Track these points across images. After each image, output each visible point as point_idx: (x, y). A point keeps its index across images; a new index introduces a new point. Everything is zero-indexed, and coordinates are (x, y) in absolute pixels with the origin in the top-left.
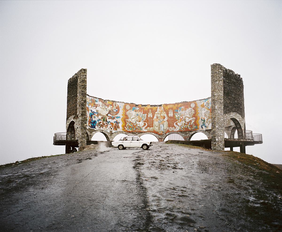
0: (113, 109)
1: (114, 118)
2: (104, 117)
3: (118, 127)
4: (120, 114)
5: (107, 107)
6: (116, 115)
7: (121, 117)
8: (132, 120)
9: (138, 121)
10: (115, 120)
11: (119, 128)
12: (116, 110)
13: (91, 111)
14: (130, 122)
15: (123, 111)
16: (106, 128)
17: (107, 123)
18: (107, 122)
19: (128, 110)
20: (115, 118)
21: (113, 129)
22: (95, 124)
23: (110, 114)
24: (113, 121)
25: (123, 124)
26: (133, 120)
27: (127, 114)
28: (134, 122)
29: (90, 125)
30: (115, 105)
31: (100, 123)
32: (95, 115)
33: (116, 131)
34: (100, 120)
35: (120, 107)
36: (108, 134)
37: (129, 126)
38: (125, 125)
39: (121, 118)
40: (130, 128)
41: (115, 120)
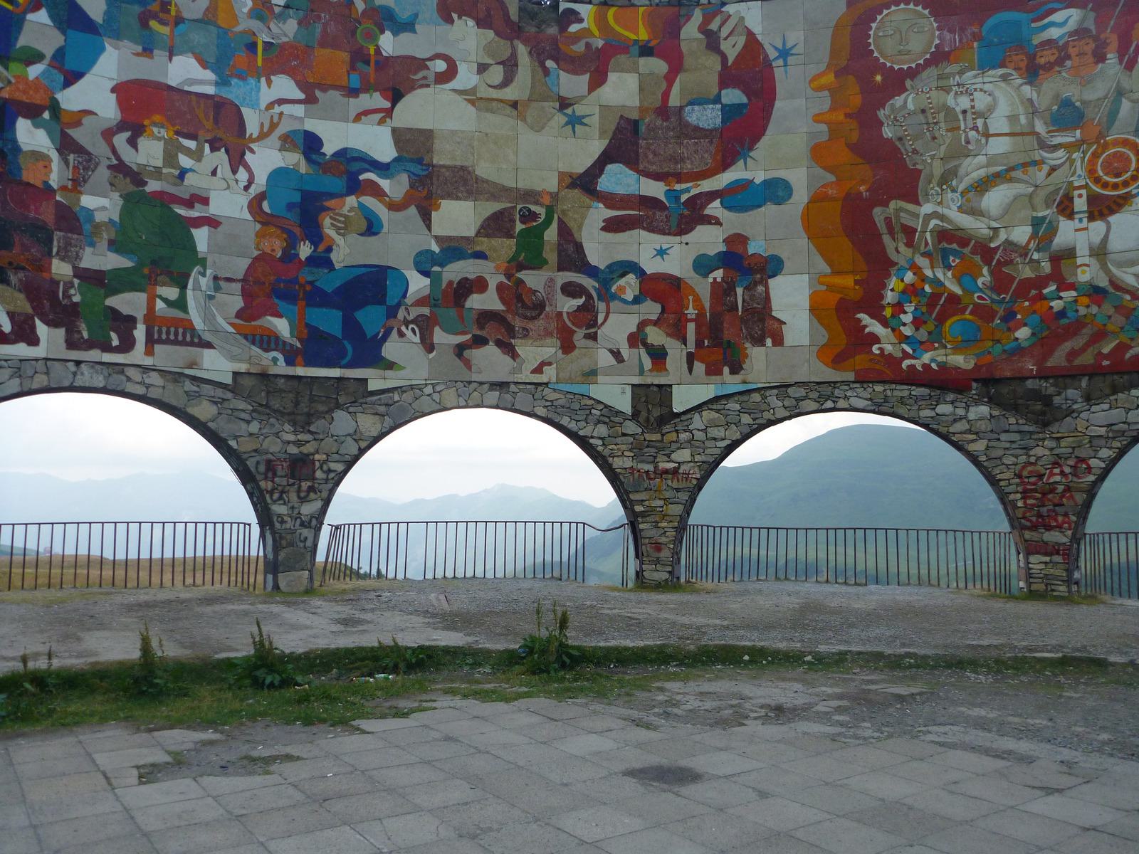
0: (674, 101)
1: (691, 216)
2: (529, 216)
3: (764, 326)
4: (789, 149)
5: (571, 84)
6: (725, 165)
7: (801, 179)
8: (976, 212)
9: (1080, 204)
10: (708, 240)
11: (779, 341)
12: (724, 106)
13: (311, 144)
14: (943, 235)
15: (827, 105)
16: (568, 347)
17: (589, 283)
18: (592, 271)
19: (913, 73)
20: (715, 208)
21: (676, 353)
22: (369, 318)
23: (632, 162)
24: (669, 256)
25: (836, 272)
26: (995, 199)
27: (888, 132)
28: (1021, 234)
29: (282, 326)
30: (712, 40)
31: (467, 287)
32: (369, 201)
33: (731, 383)
34: (454, 249)
35: (784, 53)
36: (602, 430)
37: (935, 297)
38: (856, 293)
39: (801, 196)
40: (941, 320)
41: (708, 240)
